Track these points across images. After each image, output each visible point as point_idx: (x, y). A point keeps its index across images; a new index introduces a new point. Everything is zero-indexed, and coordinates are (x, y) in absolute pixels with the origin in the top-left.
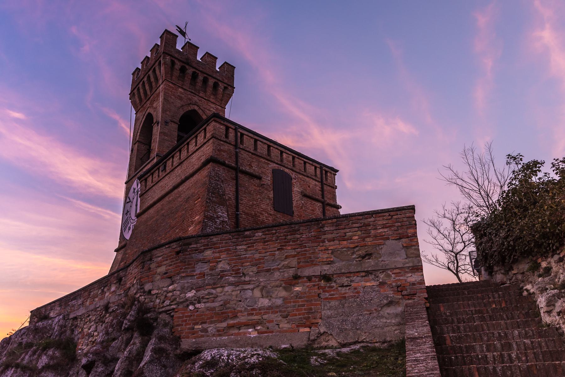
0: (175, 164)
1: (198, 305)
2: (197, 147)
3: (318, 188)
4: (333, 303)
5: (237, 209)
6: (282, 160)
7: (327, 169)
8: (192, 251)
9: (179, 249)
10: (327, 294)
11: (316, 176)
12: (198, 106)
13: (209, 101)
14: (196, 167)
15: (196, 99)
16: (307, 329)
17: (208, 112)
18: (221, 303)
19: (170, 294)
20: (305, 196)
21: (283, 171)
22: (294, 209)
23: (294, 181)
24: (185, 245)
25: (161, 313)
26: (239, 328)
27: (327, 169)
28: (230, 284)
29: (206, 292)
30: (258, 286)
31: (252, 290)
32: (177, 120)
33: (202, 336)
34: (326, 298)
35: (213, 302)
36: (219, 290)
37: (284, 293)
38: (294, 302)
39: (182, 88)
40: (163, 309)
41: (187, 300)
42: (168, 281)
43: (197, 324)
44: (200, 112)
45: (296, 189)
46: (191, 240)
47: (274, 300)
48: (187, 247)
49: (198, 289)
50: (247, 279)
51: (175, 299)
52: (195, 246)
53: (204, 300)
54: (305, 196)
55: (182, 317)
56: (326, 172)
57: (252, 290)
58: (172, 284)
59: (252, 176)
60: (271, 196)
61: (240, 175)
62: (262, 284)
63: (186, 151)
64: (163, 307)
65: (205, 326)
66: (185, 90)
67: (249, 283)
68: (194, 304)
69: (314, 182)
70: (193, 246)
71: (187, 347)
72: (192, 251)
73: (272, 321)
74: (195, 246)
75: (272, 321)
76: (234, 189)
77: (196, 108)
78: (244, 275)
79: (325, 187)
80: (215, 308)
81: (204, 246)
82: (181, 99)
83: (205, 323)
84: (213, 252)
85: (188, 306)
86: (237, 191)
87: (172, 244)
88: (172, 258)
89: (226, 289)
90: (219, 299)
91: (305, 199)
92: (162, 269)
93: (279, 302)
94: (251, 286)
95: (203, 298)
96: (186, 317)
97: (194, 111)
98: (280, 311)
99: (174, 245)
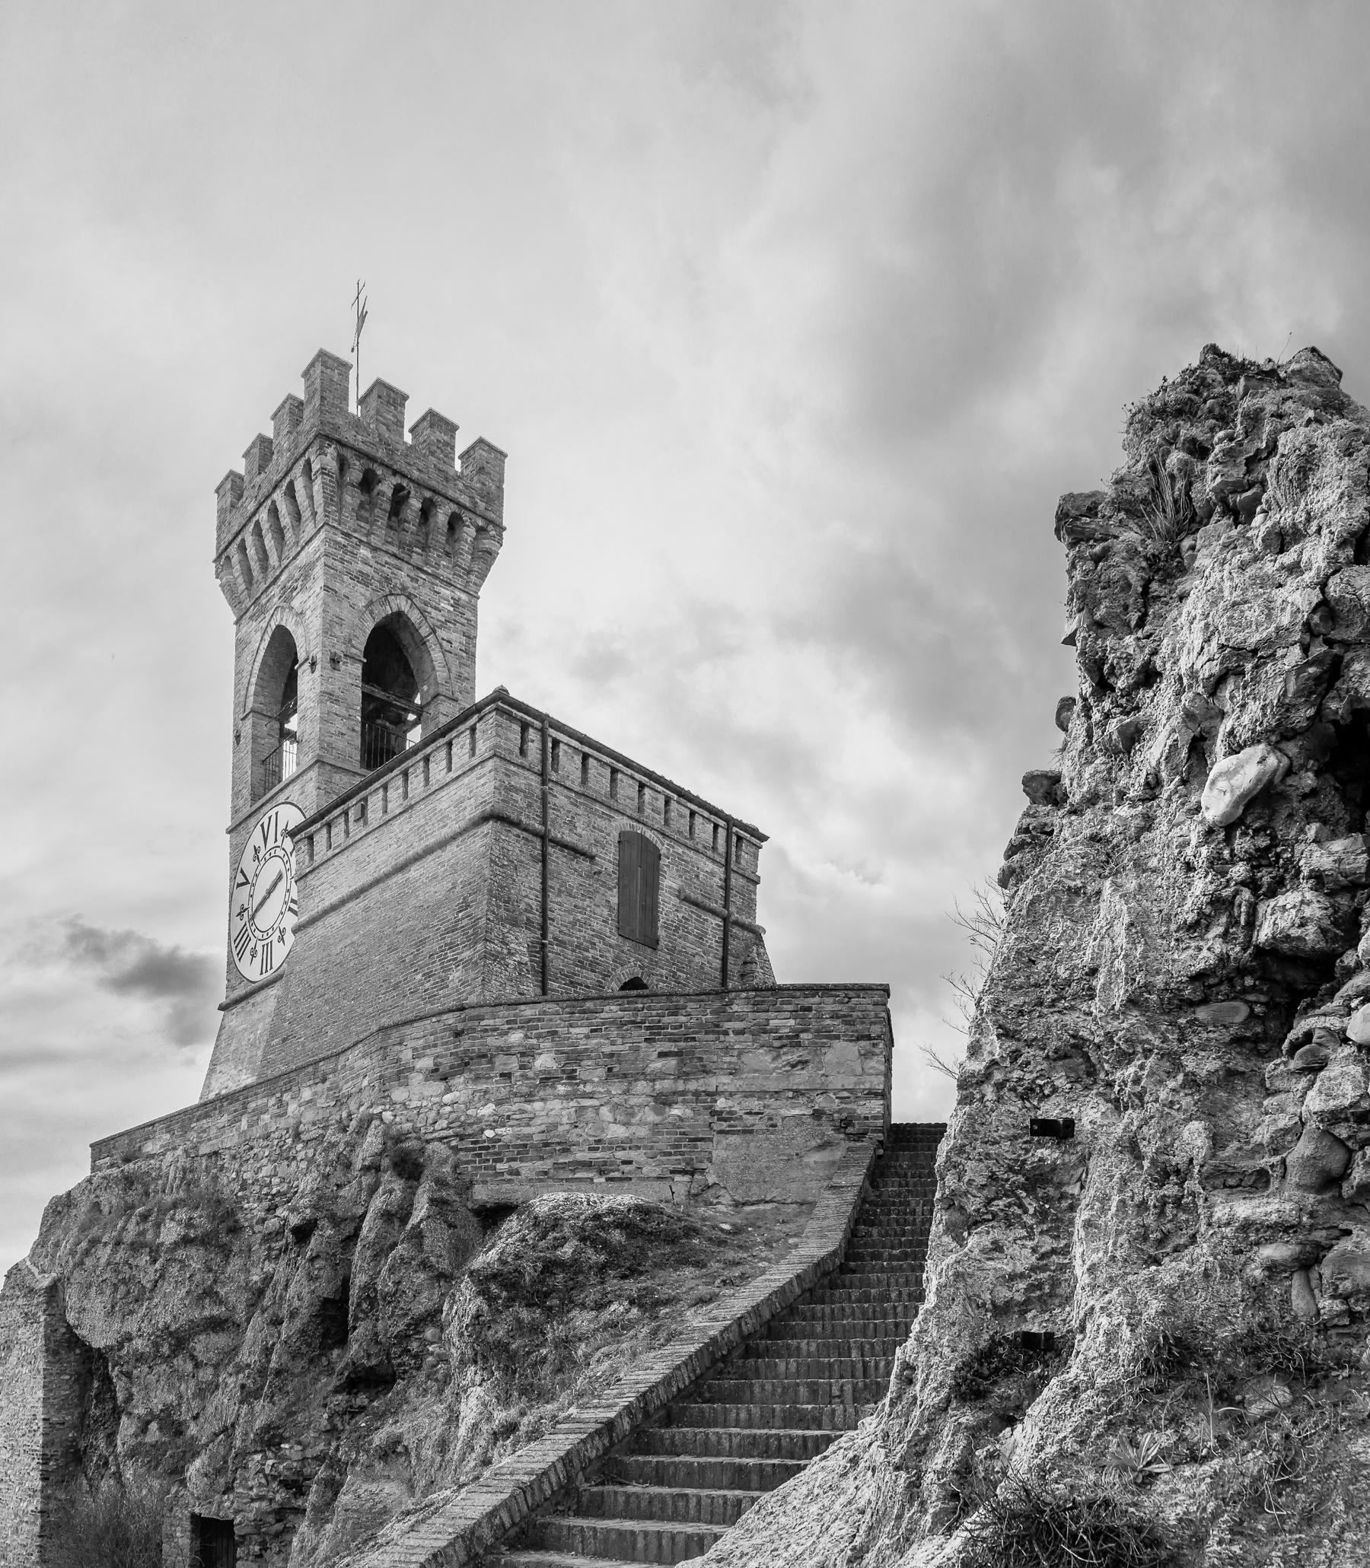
0: (394, 806)
1: (499, 1131)
2: (453, 775)
3: (717, 881)
4: (733, 1139)
5: (544, 936)
6: (640, 809)
7: (742, 833)
8: (486, 1031)
9: (460, 1027)
10: (724, 1125)
11: (714, 849)
12: (409, 597)
13: (437, 578)
14: (454, 827)
15: (403, 576)
16: (687, 1178)
17: (434, 613)
18: (543, 1128)
19: (448, 1109)
20: (687, 900)
21: (642, 837)
22: (661, 933)
23: (664, 861)
24: (471, 1019)
25: (428, 1142)
26: (573, 1171)
27: (742, 833)
28: (558, 1097)
29: (515, 1107)
30: (606, 1103)
31: (597, 1109)
32: (361, 642)
33: (509, 1181)
34: (721, 1132)
35: (528, 1125)
36: (538, 1105)
37: (651, 1117)
38: (668, 1133)
39: (368, 544)
40: (435, 1135)
41: (479, 1120)
42: (442, 1085)
43: (500, 1161)
44: (414, 616)
45: (670, 881)
46: (483, 1010)
47: (633, 1129)
48: (476, 1023)
49: (499, 1103)
50: (589, 1088)
51: (457, 1119)
52: (491, 1022)
53: (511, 1123)
54: (687, 900)
55: (474, 1149)
56: (740, 839)
57: (597, 1109)
58: (448, 1090)
59: (576, 852)
60: (614, 900)
61: (550, 850)
62: (615, 1100)
63: (422, 777)
64: (434, 1131)
65: (515, 1165)
66: (375, 549)
67: (590, 1096)
68: (493, 1128)
69: (710, 866)
70: (485, 1022)
71: (485, 1198)
72: (486, 1031)
73: (630, 1162)
74: (491, 1022)
75: (630, 1162)
76: (539, 887)
77: (403, 604)
78: (585, 1083)
79: (736, 881)
80: (530, 1136)
81: (508, 1022)
82: (363, 579)
83: (514, 1160)
84: (526, 1037)
85: (482, 1131)
86: (544, 891)
87: (445, 1017)
88: (446, 1043)
89: (550, 1105)
90: (539, 1121)
91: (685, 906)
92: (427, 1063)
93: (643, 1132)
94: (596, 1102)
95: (508, 1117)
96: (481, 1148)
97: (399, 614)
98: (645, 1147)
99: (450, 1019)
